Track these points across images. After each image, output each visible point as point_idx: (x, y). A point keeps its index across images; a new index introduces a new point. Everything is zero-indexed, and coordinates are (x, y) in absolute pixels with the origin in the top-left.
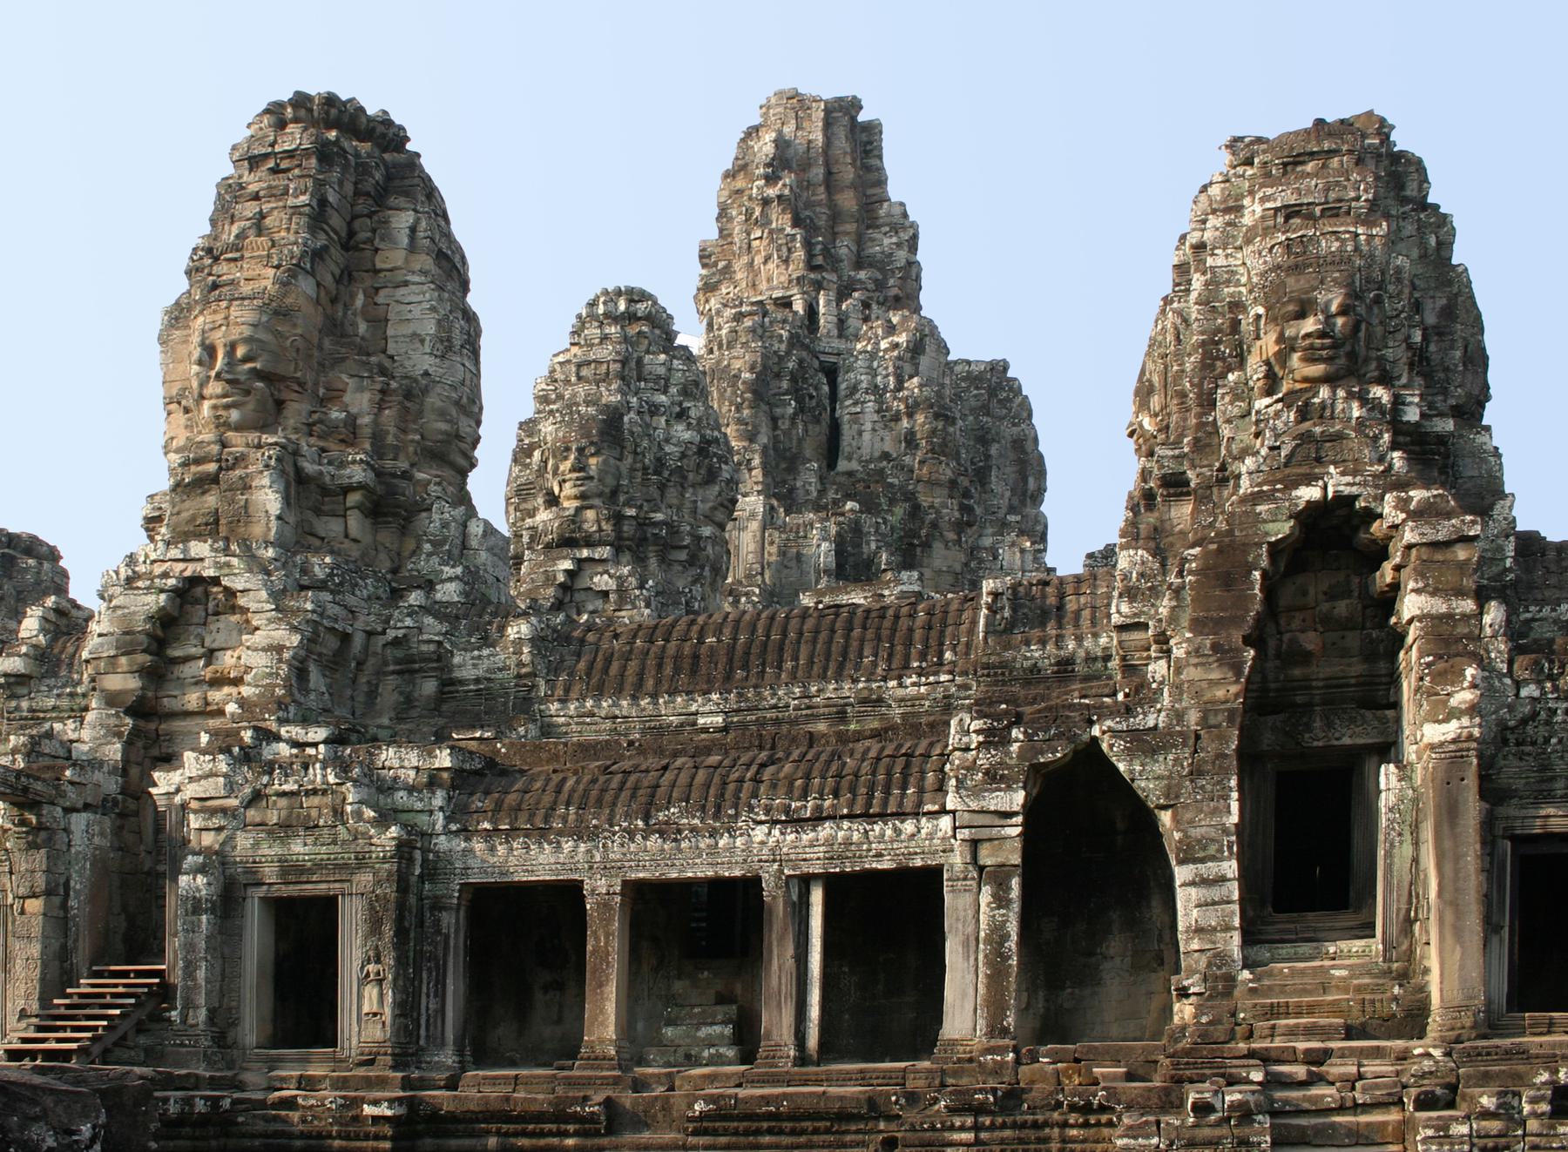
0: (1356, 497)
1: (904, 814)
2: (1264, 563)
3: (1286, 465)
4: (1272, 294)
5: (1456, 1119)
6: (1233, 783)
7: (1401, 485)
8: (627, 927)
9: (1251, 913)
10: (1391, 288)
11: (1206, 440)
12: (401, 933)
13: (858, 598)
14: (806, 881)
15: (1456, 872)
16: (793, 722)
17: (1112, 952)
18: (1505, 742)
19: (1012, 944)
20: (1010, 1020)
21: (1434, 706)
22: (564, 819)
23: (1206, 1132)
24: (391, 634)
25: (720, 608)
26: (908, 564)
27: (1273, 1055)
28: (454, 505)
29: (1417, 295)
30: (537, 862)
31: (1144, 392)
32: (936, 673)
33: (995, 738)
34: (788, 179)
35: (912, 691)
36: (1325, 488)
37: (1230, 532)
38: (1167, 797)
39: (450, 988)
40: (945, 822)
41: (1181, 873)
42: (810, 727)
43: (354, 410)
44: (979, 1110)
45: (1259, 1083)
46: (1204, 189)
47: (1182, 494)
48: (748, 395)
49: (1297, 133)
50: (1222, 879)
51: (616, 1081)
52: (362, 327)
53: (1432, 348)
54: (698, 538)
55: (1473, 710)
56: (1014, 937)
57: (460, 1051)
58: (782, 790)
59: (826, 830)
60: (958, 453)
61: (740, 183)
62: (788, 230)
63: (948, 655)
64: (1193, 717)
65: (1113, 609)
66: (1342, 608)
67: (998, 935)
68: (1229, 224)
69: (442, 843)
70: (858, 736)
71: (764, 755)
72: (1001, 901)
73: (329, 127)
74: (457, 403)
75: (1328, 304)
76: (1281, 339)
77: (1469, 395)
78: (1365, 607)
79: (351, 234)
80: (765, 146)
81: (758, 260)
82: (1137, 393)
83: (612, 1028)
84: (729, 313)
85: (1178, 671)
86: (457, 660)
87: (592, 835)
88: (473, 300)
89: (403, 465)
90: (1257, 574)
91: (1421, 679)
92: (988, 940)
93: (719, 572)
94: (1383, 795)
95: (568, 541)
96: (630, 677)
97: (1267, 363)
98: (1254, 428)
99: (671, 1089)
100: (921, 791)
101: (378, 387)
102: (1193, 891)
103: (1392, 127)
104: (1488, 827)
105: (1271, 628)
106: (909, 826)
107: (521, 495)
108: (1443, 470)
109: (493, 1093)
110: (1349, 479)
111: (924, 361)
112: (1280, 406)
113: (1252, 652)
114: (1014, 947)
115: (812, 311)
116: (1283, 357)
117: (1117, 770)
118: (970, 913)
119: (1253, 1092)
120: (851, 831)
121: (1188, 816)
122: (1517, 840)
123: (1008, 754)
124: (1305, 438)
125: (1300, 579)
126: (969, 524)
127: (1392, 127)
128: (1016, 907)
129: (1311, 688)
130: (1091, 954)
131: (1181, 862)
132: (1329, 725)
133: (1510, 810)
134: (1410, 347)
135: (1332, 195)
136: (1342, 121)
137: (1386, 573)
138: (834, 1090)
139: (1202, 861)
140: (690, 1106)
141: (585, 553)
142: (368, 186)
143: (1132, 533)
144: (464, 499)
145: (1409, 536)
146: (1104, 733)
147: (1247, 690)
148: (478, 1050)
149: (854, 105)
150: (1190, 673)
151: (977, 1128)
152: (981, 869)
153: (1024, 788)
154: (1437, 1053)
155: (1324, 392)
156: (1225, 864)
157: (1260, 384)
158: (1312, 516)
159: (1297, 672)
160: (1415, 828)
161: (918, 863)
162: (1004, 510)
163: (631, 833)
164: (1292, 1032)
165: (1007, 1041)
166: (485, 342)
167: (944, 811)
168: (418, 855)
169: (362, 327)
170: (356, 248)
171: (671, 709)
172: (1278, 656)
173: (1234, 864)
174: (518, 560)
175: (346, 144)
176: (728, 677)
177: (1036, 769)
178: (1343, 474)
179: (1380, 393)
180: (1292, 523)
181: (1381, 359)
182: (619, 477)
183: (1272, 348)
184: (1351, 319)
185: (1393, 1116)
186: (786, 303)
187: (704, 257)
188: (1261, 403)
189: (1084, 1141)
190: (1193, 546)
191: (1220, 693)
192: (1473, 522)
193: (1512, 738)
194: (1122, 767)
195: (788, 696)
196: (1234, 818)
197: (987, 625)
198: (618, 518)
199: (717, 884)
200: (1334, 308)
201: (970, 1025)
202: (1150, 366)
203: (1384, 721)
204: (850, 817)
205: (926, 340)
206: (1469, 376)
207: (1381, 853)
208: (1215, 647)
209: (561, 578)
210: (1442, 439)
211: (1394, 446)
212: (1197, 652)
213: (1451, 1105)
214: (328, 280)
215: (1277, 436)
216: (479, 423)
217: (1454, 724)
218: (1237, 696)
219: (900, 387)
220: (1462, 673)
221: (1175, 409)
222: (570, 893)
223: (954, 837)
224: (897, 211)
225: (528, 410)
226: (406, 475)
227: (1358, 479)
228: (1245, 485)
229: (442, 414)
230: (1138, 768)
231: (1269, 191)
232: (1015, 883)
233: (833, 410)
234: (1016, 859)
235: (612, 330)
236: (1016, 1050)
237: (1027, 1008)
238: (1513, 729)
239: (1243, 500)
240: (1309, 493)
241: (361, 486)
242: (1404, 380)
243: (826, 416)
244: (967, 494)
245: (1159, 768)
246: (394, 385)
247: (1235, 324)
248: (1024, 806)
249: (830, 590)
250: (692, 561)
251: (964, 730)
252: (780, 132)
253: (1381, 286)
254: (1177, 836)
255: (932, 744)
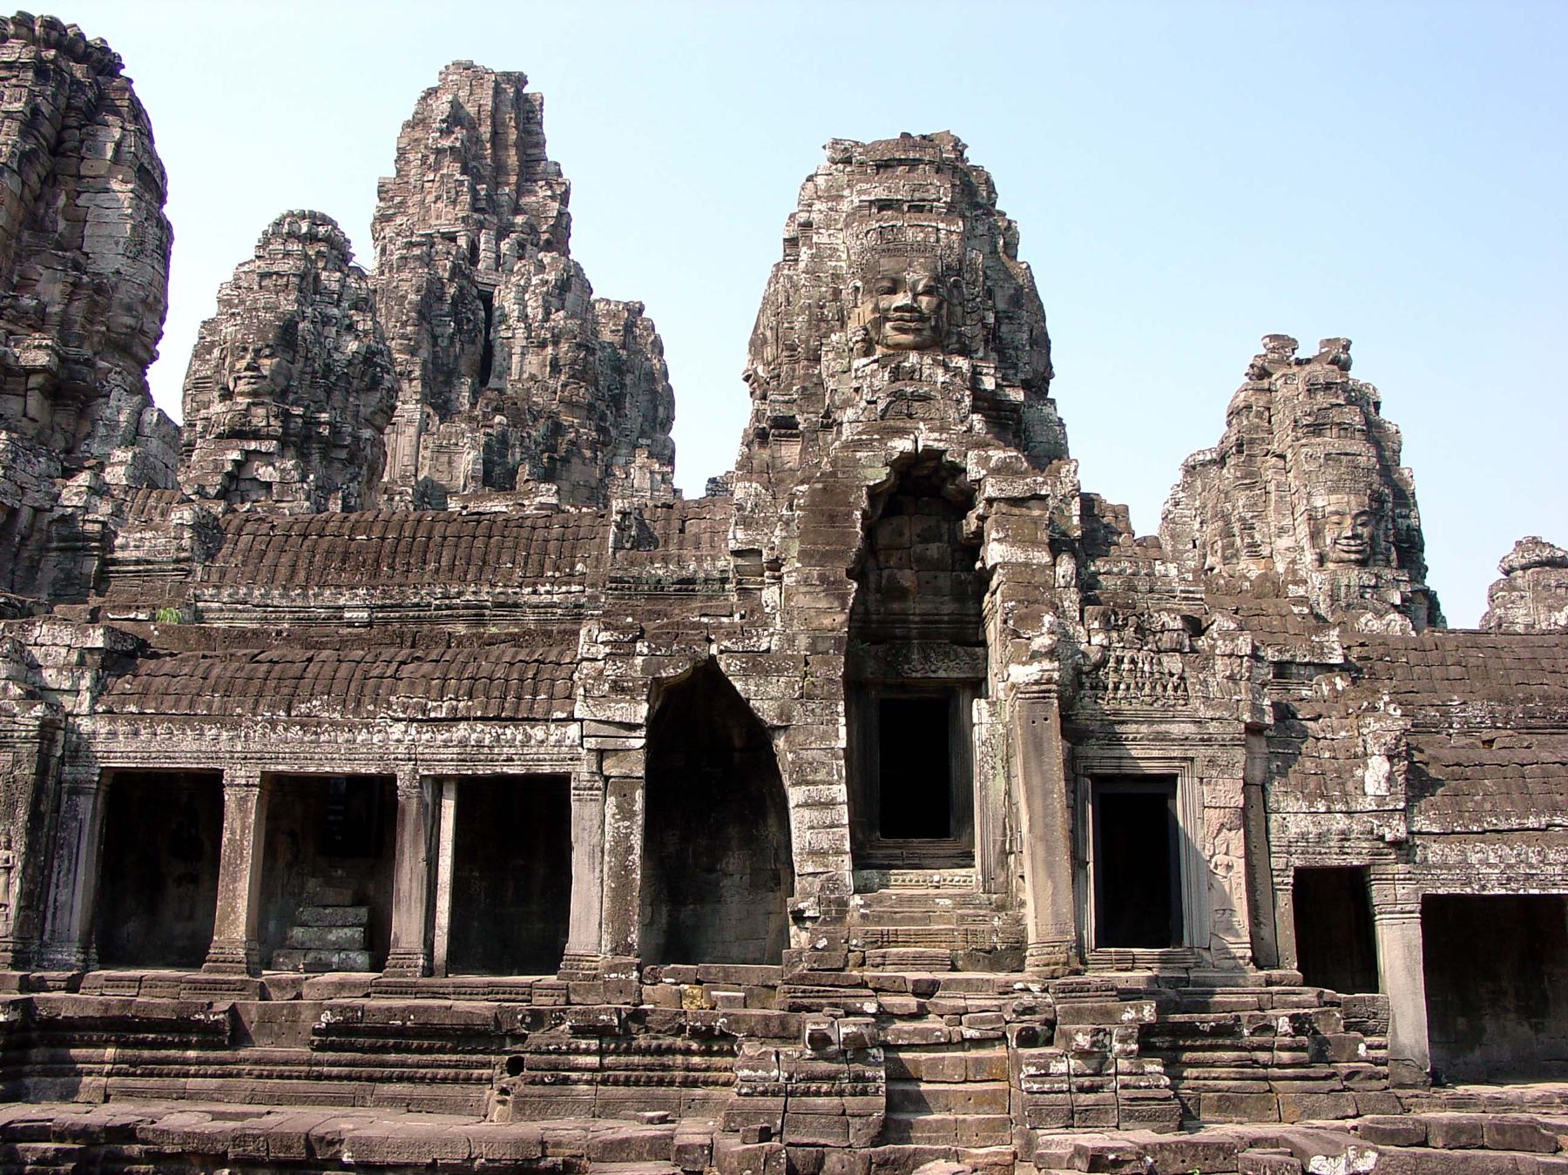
0: (944, 452)
1: (534, 720)
2: (864, 504)
3: (882, 418)
4: (867, 271)
5: (1054, 1056)
6: (841, 708)
7: (982, 445)
8: (264, 822)
9: (860, 836)
10: (967, 276)
11: (813, 392)
12: (35, 817)
13: (498, 505)
14: (439, 782)
15: (1045, 807)
16: (435, 621)
17: (731, 868)
18: (1081, 685)
19: (636, 856)
20: (634, 937)
21: (1018, 647)
22: (210, 707)
23: (823, 1066)
24: (58, 512)
25: (375, 505)
26: (548, 476)
27: (887, 985)
28: (131, 392)
29: (989, 283)
30: (183, 748)
31: (757, 345)
32: (568, 584)
33: (621, 651)
34: (459, 133)
35: (546, 599)
36: (916, 441)
37: (833, 474)
38: (780, 718)
39: (81, 877)
40: (573, 730)
41: (795, 795)
42: (448, 628)
43: (45, 299)
44: (601, 1032)
45: (873, 1015)
46: (810, 179)
47: (792, 435)
48: (413, 314)
49: (888, 142)
50: (831, 804)
51: (242, 987)
52: (62, 225)
53: (1004, 328)
54: (357, 439)
55: (1051, 654)
56: (638, 850)
57: (85, 949)
58: (420, 690)
59: (461, 730)
60: (596, 380)
61: (418, 134)
62: (458, 176)
63: (579, 567)
64: (803, 642)
65: (730, 535)
66: (934, 550)
67: (622, 842)
68: (831, 209)
69: (86, 725)
70: (493, 641)
71: (406, 651)
72: (625, 813)
73: (49, 47)
74: (144, 301)
75: (915, 284)
76: (876, 309)
77: (1035, 371)
78: (954, 551)
79: (60, 141)
80: (442, 107)
81: (431, 198)
82: (752, 343)
83: (242, 928)
84: (400, 241)
85: (788, 598)
86: (119, 541)
87: (236, 726)
88: (168, 211)
89: (87, 352)
90: (858, 514)
91: (1005, 622)
92: (613, 851)
93: (375, 471)
94: (976, 728)
95: (238, 433)
96: (283, 571)
97: (865, 329)
98: (856, 382)
99: (299, 996)
100: (551, 697)
101: (70, 280)
102: (806, 813)
103: (965, 146)
104: (1071, 762)
105: (871, 563)
106: (538, 732)
107: (196, 387)
108: (1016, 434)
109: (114, 996)
110: (936, 435)
111: (570, 298)
112: (875, 366)
113: (855, 585)
114: (637, 860)
115: (474, 248)
116: (878, 324)
117: (734, 688)
118: (596, 822)
119: (867, 1025)
120: (484, 733)
121: (801, 738)
122: (1098, 780)
123: (633, 665)
124: (898, 396)
125: (896, 521)
126: (605, 444)
127: (965, 146)
128: (640, 819)
129: (905, 621)
130: (711, 870)
131: (794, 785)
132: (926, 658)
133: (1092, 749)
134: (985, 326)
135: (917, 195)
136: (924, 137)
137: (971, 523)
138: (462, 1005)
139: (814, 783)
140: (317, 1018)
141: (253, 445)
142: (80, 101)
143: (746, 466)
144: (143, 389)
145: (990, 491)
146: (721, 652)
147: (850, 619)
148: (108, 947)
149: (521, 80)
150: (801, 600)
151: (601, 1052)
152: (607, 778)
153: (647, 701)
154: (1035, 988)
155: (913, 358)
156: (835, 788)
157: (859, 345)
158: (906, 467)
159: (896, 606)
160: (1007, 760)
161: (547, 770)
162: (636, 434)
163: (273, 724)
164: (901, 962)
165: (631, 959)
166: (176, 249)
167: (571, 719)
168: (60, 735)
169: (62, 225)
170: (64, 155)
171: (322, 600)
172: (878, 590)
173: (843, 787)
174: (191, 446)
175: (63, 64)
176: (376, 574)
177: (657, 681)
178: (931, 430)
179: (962, 363)
180: (888, 469)
181: (960, 334)
182: (289, 378)
183: (869, 317)
184: (935, 301)
185: (998, 1052)
186: (452, 238)
187: (382, 191)
188: (859, 363)
189: (708, 1069)
190: (802, 483)
191: (827, 622)
192: (1045, 483)
193: (1087, 682)
194: (738, 686)
195: (432, 595)
196: (843, 743)
197: (615, 541)
198: (286, 416)
199: (355, 780)
200: (920, 288)
201: (595, 939)
202: (764, 321)
203: (974, 657)
204: (482, 719)
205: (571, 284)
206: (1035, 355)
207: (976, 785)
208: (823, 579)
209: (229, 467)
210: (1015, 408)
211: (975, 409)
212: (806, 581)
213: (1049, 1042)
214: (34, 180)
215: (874, 392)
216: (162, 320)
217: (1036, 667)
218: (842, 625)
219: (546, 319)
220: (1039, 618)
221: (786, 360)
222: (208, 785)
223: (581, 745)
224: (552, 169)
225: (211, 310)
226: (89, 363)
227: (944, 436)
228: (847, 432)
229: (129, 309)
230: (753, 688)
231: (865, 186)
232: (639, 795)
233: (488, 333)
234: (640, 771)
235: (295, 247)
236: (640, 968)
237: (651, 923)
238: (1087, 674)
239: (846, 446)
240: (903, 445)
241: (44, 369)
242: (980, 354)
243: (481, 339)
244: (603, 417)
245: (773, 690)
246: (85, 279)
247: (837, 293)
248: (647, 719)
249: (476, 496)
250: (351, 460)
251: (592, 640)
252: (456, 96)
253: (959, 273)
254: (790, 756)
255: (561, 654)
